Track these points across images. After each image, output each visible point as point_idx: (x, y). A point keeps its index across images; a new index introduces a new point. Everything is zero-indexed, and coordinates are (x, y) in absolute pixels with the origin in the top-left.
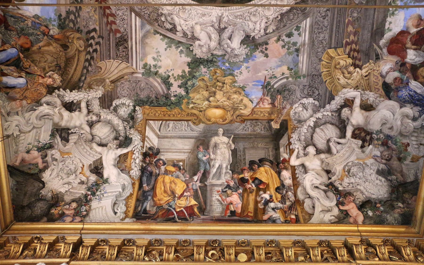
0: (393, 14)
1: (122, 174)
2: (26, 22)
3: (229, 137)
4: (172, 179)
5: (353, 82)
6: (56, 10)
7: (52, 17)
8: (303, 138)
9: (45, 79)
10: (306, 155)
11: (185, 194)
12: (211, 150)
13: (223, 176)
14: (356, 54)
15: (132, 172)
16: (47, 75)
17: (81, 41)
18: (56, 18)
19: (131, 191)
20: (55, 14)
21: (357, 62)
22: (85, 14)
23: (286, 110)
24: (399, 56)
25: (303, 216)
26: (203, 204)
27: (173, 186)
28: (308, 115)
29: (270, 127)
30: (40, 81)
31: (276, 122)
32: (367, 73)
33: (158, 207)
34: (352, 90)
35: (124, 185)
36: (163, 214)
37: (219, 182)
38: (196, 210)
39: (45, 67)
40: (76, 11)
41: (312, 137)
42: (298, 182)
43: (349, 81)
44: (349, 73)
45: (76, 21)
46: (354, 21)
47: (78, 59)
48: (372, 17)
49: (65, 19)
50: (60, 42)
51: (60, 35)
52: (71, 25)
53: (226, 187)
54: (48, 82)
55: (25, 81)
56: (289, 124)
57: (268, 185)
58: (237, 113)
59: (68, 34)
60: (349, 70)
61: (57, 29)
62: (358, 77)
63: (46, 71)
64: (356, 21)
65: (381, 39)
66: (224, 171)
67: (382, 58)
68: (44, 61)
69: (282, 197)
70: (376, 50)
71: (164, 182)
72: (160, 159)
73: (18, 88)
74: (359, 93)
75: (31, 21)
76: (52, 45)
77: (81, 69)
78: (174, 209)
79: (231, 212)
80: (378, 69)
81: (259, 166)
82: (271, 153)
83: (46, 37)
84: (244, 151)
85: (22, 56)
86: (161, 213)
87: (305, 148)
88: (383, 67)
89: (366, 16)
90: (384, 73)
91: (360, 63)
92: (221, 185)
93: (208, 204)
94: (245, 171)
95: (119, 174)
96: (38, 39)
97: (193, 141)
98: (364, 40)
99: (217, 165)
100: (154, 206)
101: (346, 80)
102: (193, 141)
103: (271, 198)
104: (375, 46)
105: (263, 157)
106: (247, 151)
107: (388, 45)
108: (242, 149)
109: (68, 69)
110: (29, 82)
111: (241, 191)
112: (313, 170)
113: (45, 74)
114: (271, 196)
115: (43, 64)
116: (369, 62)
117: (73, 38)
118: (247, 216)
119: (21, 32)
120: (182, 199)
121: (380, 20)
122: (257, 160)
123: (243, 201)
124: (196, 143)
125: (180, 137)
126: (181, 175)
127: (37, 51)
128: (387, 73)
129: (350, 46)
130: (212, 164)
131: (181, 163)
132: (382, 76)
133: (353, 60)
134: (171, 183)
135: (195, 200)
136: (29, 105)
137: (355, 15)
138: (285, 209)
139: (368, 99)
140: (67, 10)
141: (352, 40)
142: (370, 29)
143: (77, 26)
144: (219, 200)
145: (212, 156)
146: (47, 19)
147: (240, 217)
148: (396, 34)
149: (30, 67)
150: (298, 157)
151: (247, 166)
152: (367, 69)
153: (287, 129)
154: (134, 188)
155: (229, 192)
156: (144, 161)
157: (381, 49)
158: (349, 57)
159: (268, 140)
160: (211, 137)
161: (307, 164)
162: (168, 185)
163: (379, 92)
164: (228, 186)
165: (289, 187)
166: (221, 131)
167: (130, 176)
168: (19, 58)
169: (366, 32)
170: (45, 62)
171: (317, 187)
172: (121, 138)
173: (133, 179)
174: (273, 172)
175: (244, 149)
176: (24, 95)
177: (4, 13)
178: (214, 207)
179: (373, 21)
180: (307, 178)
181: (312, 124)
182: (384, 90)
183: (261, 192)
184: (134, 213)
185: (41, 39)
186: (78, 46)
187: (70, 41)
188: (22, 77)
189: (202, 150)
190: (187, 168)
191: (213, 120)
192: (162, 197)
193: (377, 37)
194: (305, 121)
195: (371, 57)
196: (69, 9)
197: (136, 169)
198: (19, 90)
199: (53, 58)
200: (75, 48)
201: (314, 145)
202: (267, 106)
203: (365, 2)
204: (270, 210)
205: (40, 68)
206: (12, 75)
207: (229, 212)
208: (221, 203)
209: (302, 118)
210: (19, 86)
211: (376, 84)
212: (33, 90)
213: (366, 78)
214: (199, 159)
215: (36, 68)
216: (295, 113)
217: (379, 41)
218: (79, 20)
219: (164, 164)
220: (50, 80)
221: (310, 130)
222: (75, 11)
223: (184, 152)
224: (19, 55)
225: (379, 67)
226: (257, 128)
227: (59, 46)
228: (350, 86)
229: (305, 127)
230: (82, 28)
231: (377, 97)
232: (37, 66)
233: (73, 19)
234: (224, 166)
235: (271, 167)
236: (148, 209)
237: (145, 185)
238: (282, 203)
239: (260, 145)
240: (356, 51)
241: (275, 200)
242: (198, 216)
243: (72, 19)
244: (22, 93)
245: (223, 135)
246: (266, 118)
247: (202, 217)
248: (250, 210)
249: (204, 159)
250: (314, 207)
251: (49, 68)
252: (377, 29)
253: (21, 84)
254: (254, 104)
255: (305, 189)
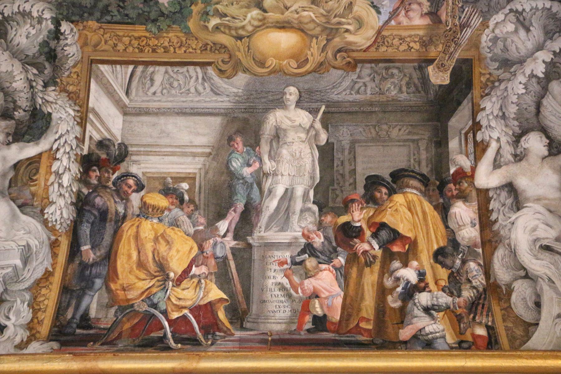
1: (24, 217)
3: (313, 112)
4: (161, 228)
8: (512, 110)
10: (519, 157)
11: (194, 270)
12: (265, 148)
13: (295, 219)
15: (50, 210)
19: (47, 264)
23: (468, 32)
25: (507, 329)
26: (241, 297)
27: (162, 248)
28: (530, 45)
29: (425, 80)
31: (441, 67)
33: (122, 309)
35: (28, 247)
36: (133, 328)
37: (284, 237)
38: (221, 315)
41: (538, 106)
42: (497, 234)
53: (303, 252)
56: (477, 70)
57: (414, 244)
58: (337, 42)
66: (298, 205)
69: (451, 276)
71: (137, 237)
72: (128, 175)
78: (165, 313)
79: (316, 319)
81: (392, 192)
82: (424, 155)
84: (352, 150)
86: (127, 326)
87: (517, 139)
92: (289, 245)
93: (255, 298)
94: (355, 206)
95: (14, 217)
97: (217, 121)
99: (280, 191)
100: (109, 306)
102: (217, 121)
103: (421, 281)
105: (402, 165)
106: (359, 150)
108: (346, 143)
111: (341, 260)
112: (538, 200)
114: (421, 275)
118: (358, 329)
120: (185, 284)
122: (385, 174)
123: (346, 287)
124: (225, 127)
125: (182, 113)
126: (183, 218)
130: (267, 185)
131: (185, 186)
134: (156, 240)
135: (221, 288)
138: (459, 311)
144: (282, 288)
145: (268, 165)
147: (337, 332)
150: (497, 165)
151: (361, 190)
153: (469, 85)
154: (55, 255)
155: (311, 263)
156: (83, 179)
159: (416, 118)
160: (267, 110)
161: (522, 183)
162: (149, 247)
164: (309, 249)
165: (471, 248)
166: (292, 93)
167: (45, 223)
171: (547, 248)
172: (18, 114)
173: (52, 230)
174: (428, 207)
175: (353, 143)
178: (271, 307)
180: (520, 223)
181: (540, 70)
183: (396, 264)
184: (54, 325)
189: (240, 147)
190: (201, 200)
191: (272, 62)
192: (132, 279)
194: (521, 62)
197: (61, 202)
201: (544, 131)
202: (418, 21)
204: (418, 312)
207: (308, 318)
208: (290, 296)
209: (513, 54)
214: (232, 175)
216: (495, 40)
219: (140, 187)
221: (535, 87)
223: (194, 155)
226: (388, 85)
229: (522, 79)
234: (299, 191)
235: (425, 194)
236: (93, 314)
237: (85, 248)
238: (451, 294)
239: (394, 133)
241: (432, 286)
242: (228, 333)
245: (299, 104)
246: (414, 56)
247: (238, 334)
248: (364, 314)
249: (247, 171)
250: (538, 305)
254: (384, 17)
255: (513, 253)
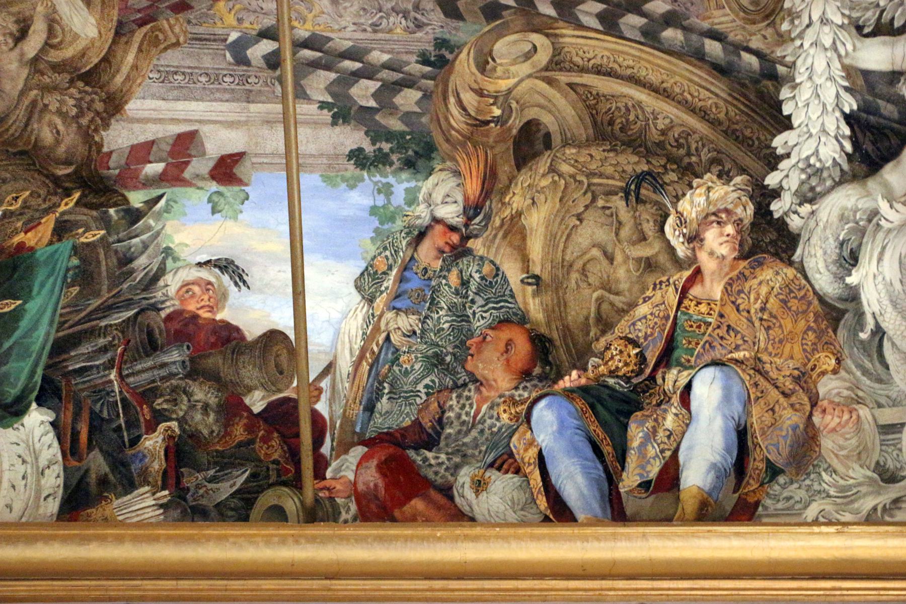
2: (395, 338)
6: (326, 179)
7: (368, 202)
9: (708, 264)
16: (682, 251)
17: (500, 47)
18: (370, 180)
20: (352, 187)
22: (347, 20)
30: (717, 291)
39: (639, 260)
40: (328, 68)
45: (385, 74)
47: (598, 71)
49: (377, 134)
50: (505, 169)
51: (463, 167)
52: (408, 99)
54: (724, 250)
55: (710, 372)
59: (457, 119)
61: (432, 180)
63: (663, 259)
68: (605, 262)
73: (749, 414)
75: (390, 315)
76: (519, 214)
77: (661, 59)
83: (477, 245)
85: (572, 379)
96: (486, 285)
109: (654, 135)
110: (718, 353)
113: (679, 264)
115: (621, 273)
117: (480, 93)
119: (448, 370)
127: (548, 298)
136: (849, 363)
140: (327, 116)
143: (416, 68)
146: (376, 231)
149: (634, 343)
168: (584, 391)
170: (611, 259)
176: (789, 385)
177: (353, 444)
185: (487, 269)
186: (525, 69)
187: (497, 112)
188: (688, 387)
196: (323, 105)
198: (756, 411)
199: (590, 216)
200: (542, 86)
205: (644, 289)
206: (676, 438)
210: (737, 408)
212: (762, 336)
215: (643, 309)
218: (378, 57)
220: (711, 236)
222: (333, 76)
224: (569, 393)
227: (524, 178)
230: (424, 40)
232: (633, 305)
233: (373, 86)
243: (375, 96)
244: (774, 394)
251: (643, 238)
253: (727, 398)
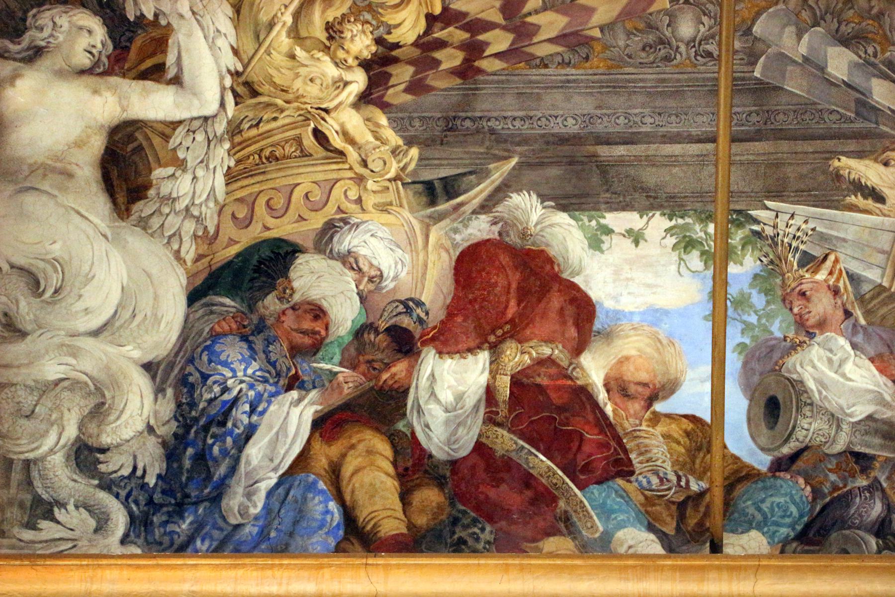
0: (688, 244)
5: (278, 58)
14: (450, 59)
21: (402, 74)
24: (452, 312)
32: (337, 142)
34: (230, 61)
43: (281, 39)
44: (333, 31)
46: (651, 27)
48: (673, 129)
60: (353, 29)
62: (313, 90)
64: (651, 38)
65: (543, 198)
67: (439, 218)
70: (481, 174)
74: (212, 108)
80: (370, 201)
88: (383, 232)
89: (677, 93)
90: (346, 241)
91: (396, 94)
98: (538, 98)
101: (288, 19)
104: (500, 172)
107: (513, 239)
116: (410, 142)
121: (651, 177)
128: (348, 260)
129: (498, 18)
132: (330, 229)
133: (416, 44)
137: (686, 28)
139: (181, 164)
141: (537, 28)
142: (600, 127)
148: (577, 280)
152: (364, 136)
157: (484, 208)
158: (431, 19)
163: (229, 230)
169: (584, 104)
179: (648, 139)
182: (245, 255)
193: (554, 172)
195: (436, 152)
203: (757, 74)
211: (279, 202)
213: (309, 141)
217: (531, 187)
225: (383, 208)
228: (248, 47)
231: (198, 219)
240: (467, 61)
252: (604, 168)
